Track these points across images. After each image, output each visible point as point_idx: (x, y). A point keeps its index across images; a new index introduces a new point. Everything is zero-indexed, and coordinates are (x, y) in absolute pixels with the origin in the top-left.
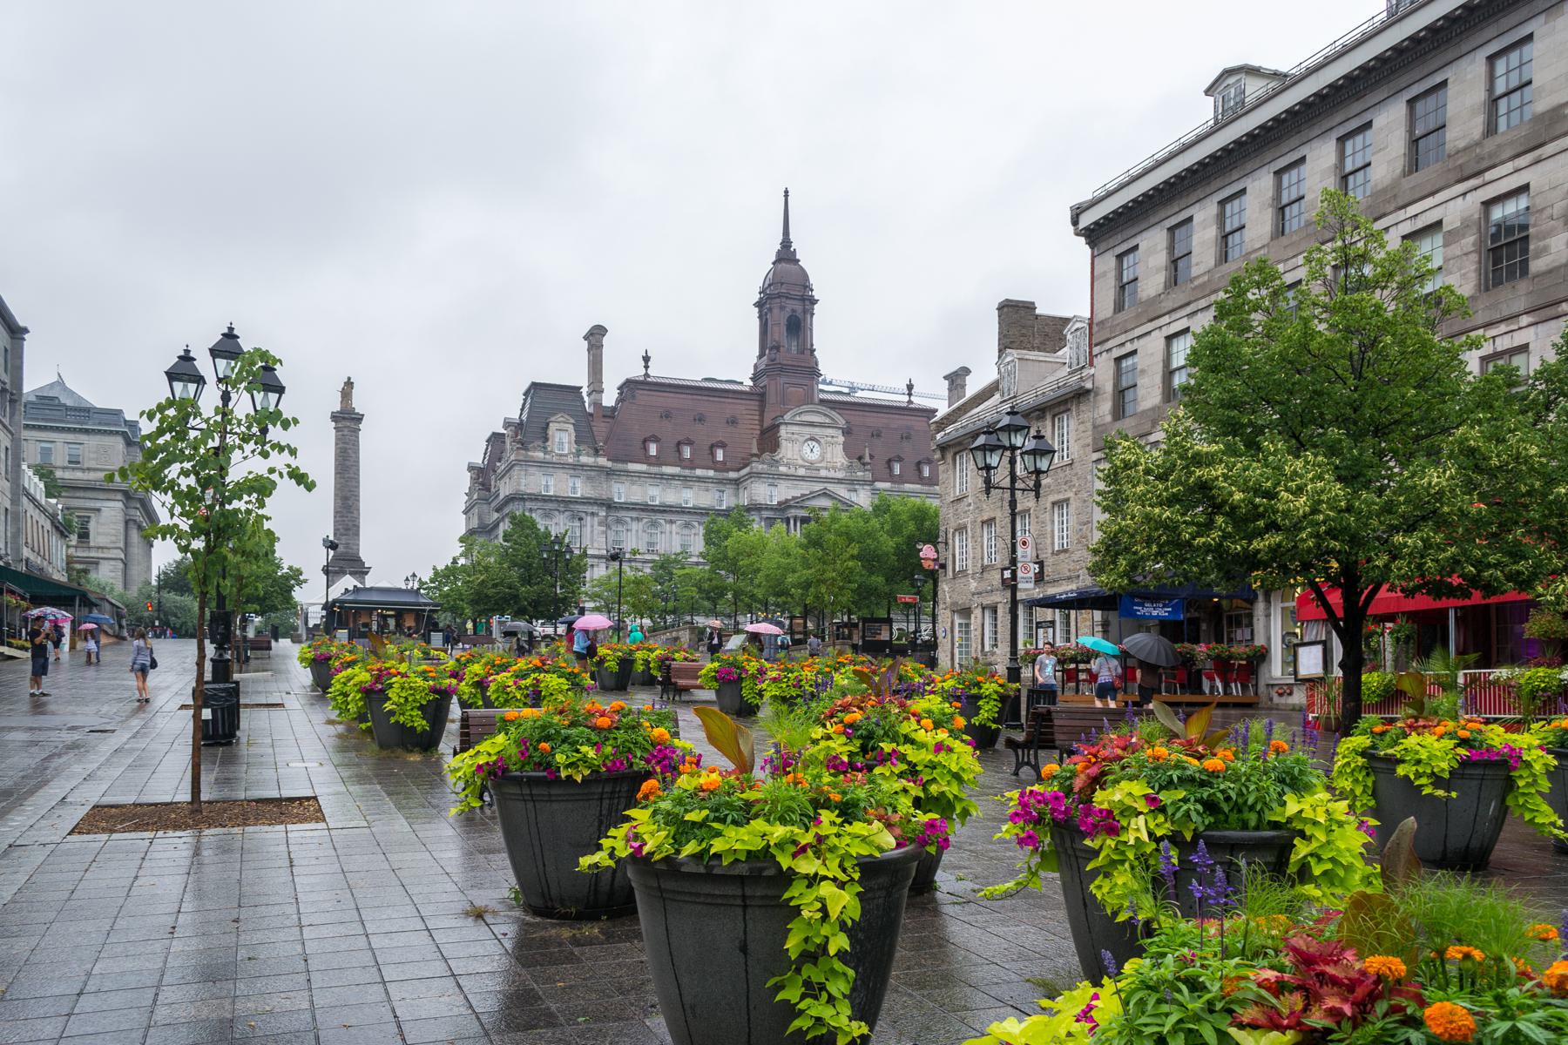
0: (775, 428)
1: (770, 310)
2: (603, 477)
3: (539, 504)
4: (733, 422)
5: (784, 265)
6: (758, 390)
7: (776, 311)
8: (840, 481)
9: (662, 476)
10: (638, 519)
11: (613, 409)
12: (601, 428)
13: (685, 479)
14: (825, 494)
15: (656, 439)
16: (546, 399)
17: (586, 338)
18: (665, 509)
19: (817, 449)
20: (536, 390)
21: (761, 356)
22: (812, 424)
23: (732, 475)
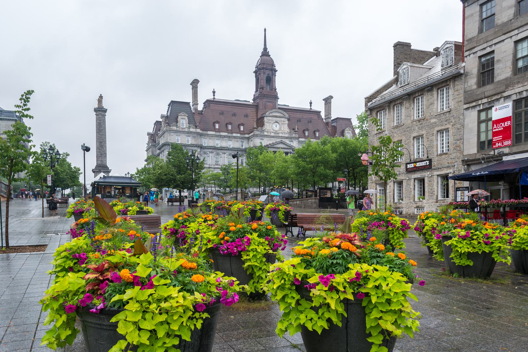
0: (262, 118)
1: (260, 74)
2: (199, 136)
4: (246, 116)
5: (265, 57)
6: (256, 104)
7: (262, 74)
8: (287, 138)
9: (221, 136)
10: (212, 152)
11: (202, 111)
12: (197, 118)
14: (282, 143)
15: (218, 122)
17: (191, 84)
18: (222, 149)
19: (278, 126)
20: (173, 103)
21: (256, 91)
22: (276, 117)
23: (247, 136)
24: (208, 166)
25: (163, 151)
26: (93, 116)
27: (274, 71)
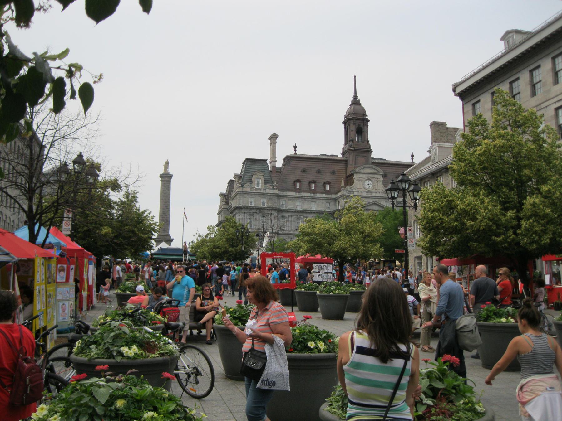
1: (349, 125)
2: (276, 198)
3: (248, 210)
4: (333, 173)
6: (345, 159)
7: (352, 125)
11: (281, 168)
12: (275, 176)
13: (313, 198)
14: (375, 204)
15: (299, 181)
16: (253, 165)
20: (248, 161)
21: (345, 144)
23: (333, 196)
24: (287, 232)
25: (235, 215)
26: (158, 183)
27: (366, 121)
